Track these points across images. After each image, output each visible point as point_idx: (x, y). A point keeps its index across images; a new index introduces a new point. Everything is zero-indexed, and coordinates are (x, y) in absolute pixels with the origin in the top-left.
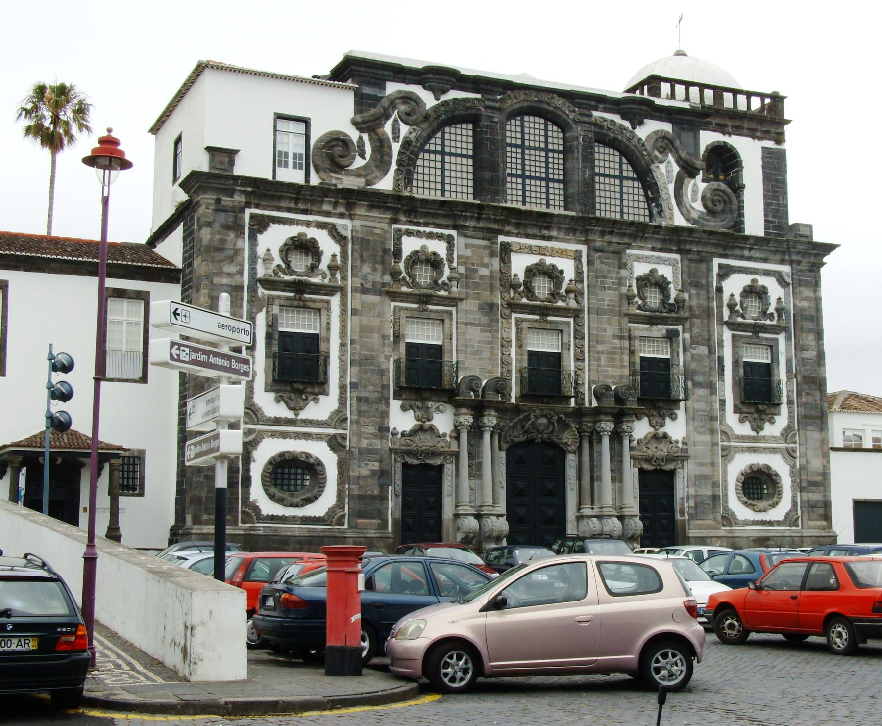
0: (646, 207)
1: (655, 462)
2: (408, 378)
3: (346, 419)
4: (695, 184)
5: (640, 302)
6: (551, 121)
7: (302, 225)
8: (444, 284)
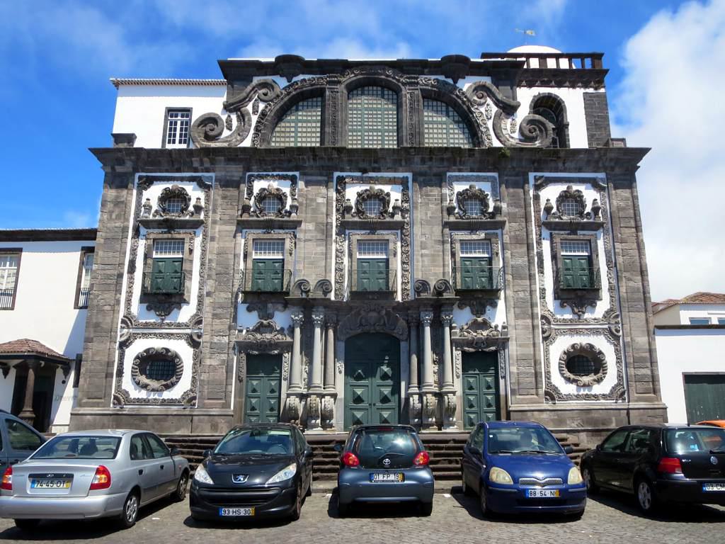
1: (476, 344)
7: (177, 181)
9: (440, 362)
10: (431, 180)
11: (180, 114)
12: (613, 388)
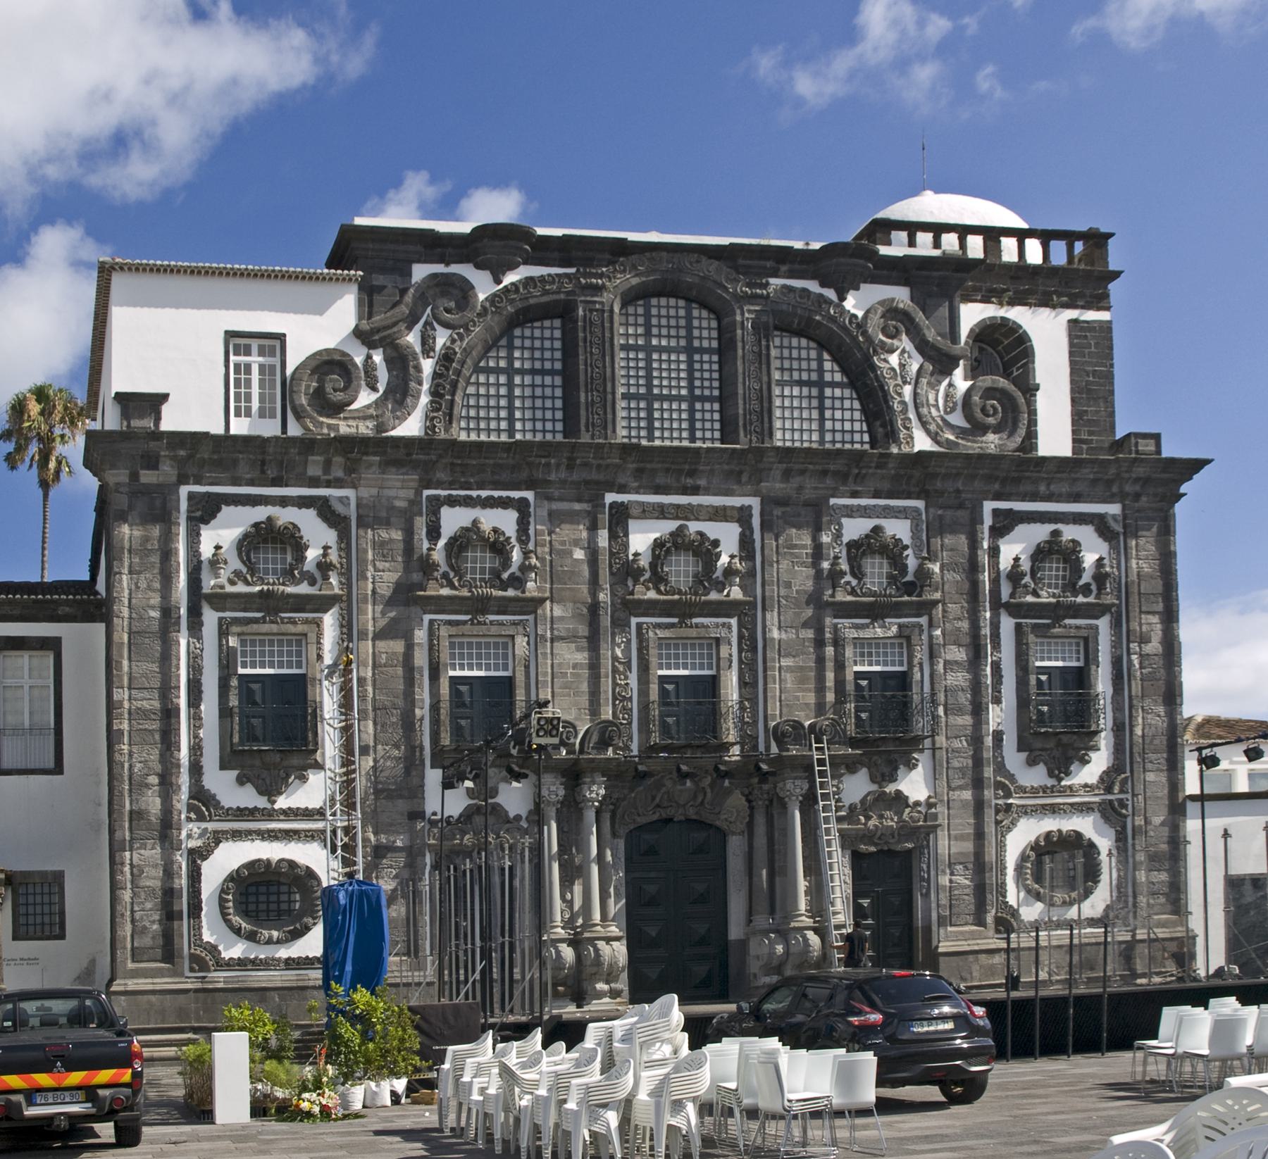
0: (865, 428)
2: (457, 731)
4: (950, 385)
5: (854, 582)
7: (274, 504)
10: (799, 515)
11: (255, 344)
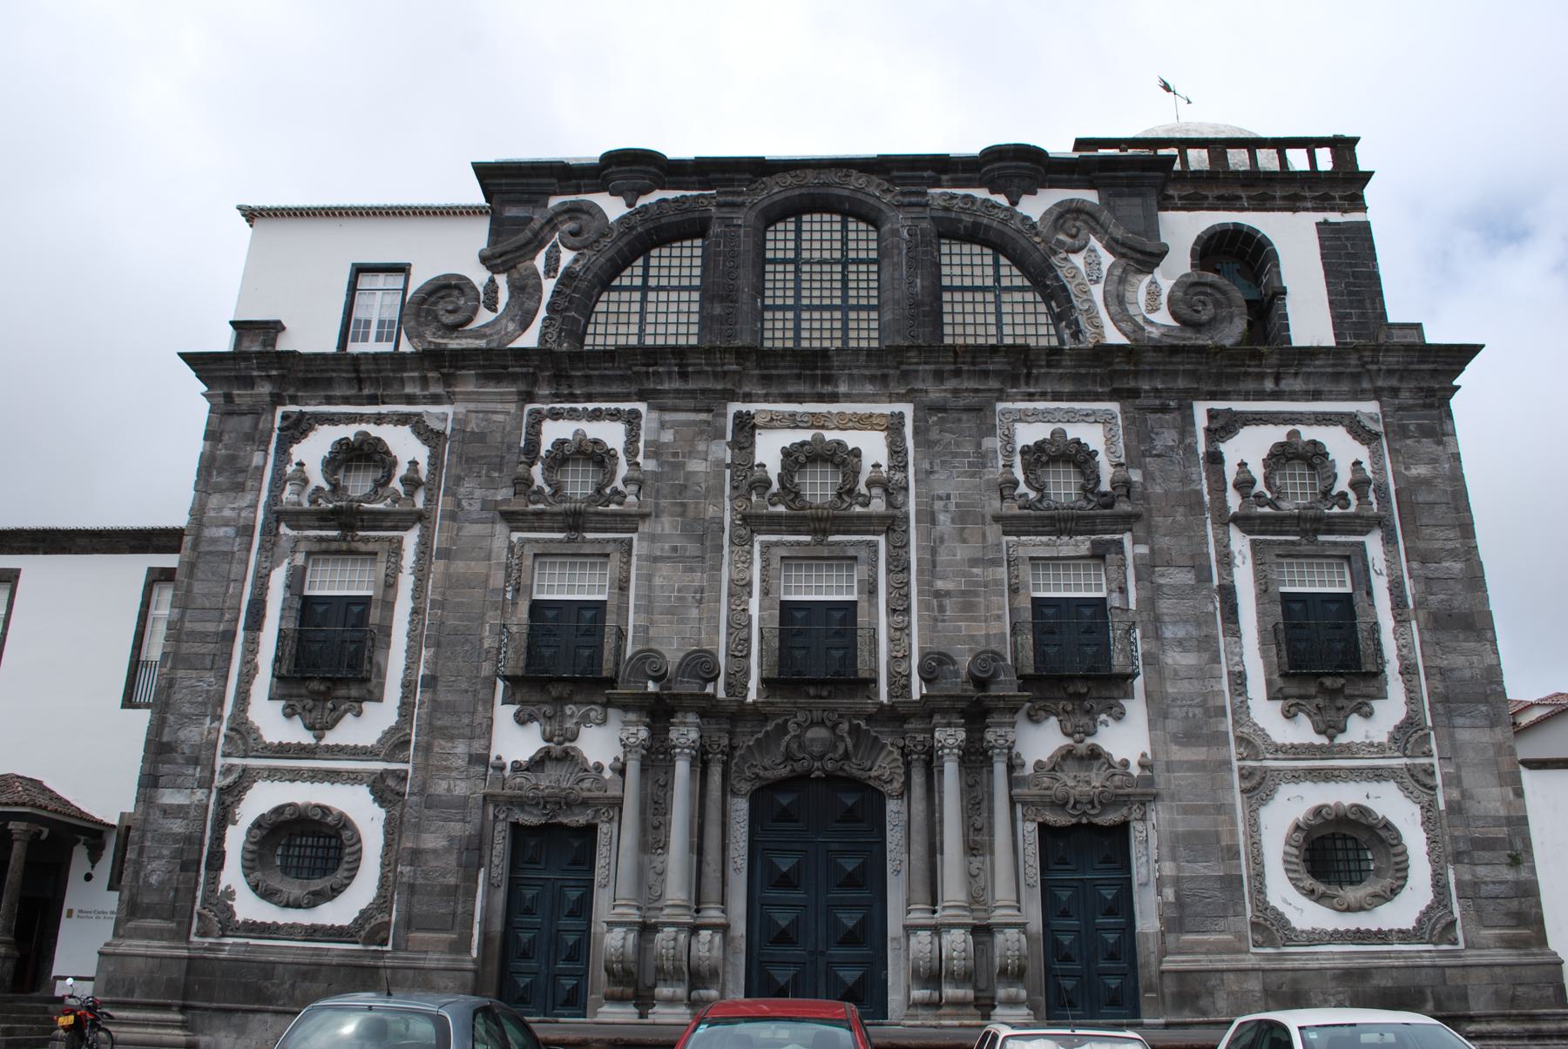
0: (1052, 331)
1: (1074, 807)
3: (409, 742)
5: (1032, 495)
6: (853, 216)
7: (368, 422)
8: (616, 492)
9: (977, 844)
10: (960, 420)
12: (1423, 914)
